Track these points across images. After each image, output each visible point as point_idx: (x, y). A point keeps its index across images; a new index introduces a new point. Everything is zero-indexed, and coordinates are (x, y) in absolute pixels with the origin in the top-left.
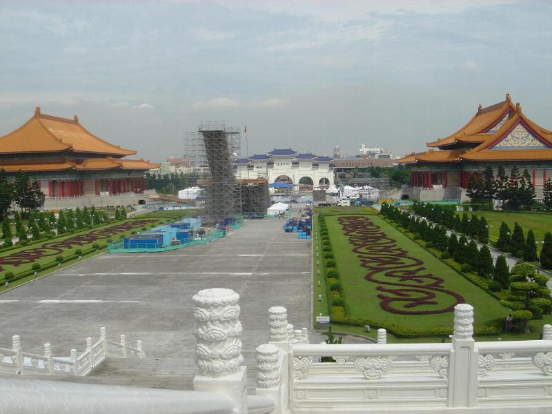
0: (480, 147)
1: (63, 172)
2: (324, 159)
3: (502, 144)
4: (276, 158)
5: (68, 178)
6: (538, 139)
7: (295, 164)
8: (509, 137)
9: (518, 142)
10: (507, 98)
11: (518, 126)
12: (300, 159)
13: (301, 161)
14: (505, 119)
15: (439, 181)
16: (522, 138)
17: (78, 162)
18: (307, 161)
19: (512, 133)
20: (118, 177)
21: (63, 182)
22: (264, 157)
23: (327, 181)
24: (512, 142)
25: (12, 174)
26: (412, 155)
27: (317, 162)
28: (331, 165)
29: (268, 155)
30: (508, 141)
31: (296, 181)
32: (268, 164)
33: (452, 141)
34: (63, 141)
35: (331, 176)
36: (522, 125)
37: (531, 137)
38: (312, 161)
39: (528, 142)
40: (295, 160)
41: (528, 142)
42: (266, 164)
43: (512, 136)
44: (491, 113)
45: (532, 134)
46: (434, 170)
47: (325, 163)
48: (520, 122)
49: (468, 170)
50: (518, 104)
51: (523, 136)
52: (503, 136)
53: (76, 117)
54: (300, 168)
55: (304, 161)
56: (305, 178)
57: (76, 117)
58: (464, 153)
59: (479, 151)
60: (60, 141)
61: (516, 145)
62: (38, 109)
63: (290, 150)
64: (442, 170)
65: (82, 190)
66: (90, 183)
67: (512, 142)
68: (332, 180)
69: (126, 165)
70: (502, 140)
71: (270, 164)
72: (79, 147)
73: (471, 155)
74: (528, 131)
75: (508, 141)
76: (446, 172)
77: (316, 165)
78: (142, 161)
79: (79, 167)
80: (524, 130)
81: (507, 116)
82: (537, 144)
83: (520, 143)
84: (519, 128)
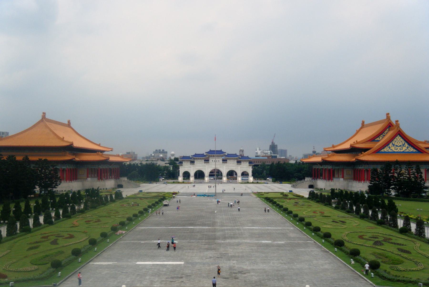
3: (386, 149)
4: (211, 156)
5: (67, 167)
7: (225, 161)
8: (391, 145)
10: (387, 116)
11: (397, 137)
13: (229, 159)
14: (386, 132)
16: (400, 146)
18: (233, 159)
19: (393, 142)
20: (104, 167)
21: (63, 170)
22: (203, 155)
24: (393, 148)
25: (33, 162)
27: (240, 159)
28: (250, 163)
30: (390, 148)
31: (225, 173)
32: (205, 161)
34: (65, 139)
35: (250, 170)
36: (400, 136)
37: (406, 145)
38: (236, 159)
39: (404, 148)
41: (404, 148)
42: (203, 160)
43: (393, 144)
45: (407, 142)
46: (330, 167)
47: (246, 161)
48: (399, 134)
49: (357, 168)
51: (401, 144)
52: (387, 144)
54: (228, 164)
55: (231, 159)
56: (230, 171)
58: (358, 155)
60: (63, 139)
62: (44, 113)
63: (221, 151)
66: (83, 172)
67: (393, 148)
68: (250, 173)
70: (386, 147)
71: (207, 161)
75: (390, 148)
77: (239, 162)
78: (118, 156)
79: (77, 159)
80: (402, 140)
81: (388, 129)
82: (412, 149)
83: (399, 149)
84: (399, 138)
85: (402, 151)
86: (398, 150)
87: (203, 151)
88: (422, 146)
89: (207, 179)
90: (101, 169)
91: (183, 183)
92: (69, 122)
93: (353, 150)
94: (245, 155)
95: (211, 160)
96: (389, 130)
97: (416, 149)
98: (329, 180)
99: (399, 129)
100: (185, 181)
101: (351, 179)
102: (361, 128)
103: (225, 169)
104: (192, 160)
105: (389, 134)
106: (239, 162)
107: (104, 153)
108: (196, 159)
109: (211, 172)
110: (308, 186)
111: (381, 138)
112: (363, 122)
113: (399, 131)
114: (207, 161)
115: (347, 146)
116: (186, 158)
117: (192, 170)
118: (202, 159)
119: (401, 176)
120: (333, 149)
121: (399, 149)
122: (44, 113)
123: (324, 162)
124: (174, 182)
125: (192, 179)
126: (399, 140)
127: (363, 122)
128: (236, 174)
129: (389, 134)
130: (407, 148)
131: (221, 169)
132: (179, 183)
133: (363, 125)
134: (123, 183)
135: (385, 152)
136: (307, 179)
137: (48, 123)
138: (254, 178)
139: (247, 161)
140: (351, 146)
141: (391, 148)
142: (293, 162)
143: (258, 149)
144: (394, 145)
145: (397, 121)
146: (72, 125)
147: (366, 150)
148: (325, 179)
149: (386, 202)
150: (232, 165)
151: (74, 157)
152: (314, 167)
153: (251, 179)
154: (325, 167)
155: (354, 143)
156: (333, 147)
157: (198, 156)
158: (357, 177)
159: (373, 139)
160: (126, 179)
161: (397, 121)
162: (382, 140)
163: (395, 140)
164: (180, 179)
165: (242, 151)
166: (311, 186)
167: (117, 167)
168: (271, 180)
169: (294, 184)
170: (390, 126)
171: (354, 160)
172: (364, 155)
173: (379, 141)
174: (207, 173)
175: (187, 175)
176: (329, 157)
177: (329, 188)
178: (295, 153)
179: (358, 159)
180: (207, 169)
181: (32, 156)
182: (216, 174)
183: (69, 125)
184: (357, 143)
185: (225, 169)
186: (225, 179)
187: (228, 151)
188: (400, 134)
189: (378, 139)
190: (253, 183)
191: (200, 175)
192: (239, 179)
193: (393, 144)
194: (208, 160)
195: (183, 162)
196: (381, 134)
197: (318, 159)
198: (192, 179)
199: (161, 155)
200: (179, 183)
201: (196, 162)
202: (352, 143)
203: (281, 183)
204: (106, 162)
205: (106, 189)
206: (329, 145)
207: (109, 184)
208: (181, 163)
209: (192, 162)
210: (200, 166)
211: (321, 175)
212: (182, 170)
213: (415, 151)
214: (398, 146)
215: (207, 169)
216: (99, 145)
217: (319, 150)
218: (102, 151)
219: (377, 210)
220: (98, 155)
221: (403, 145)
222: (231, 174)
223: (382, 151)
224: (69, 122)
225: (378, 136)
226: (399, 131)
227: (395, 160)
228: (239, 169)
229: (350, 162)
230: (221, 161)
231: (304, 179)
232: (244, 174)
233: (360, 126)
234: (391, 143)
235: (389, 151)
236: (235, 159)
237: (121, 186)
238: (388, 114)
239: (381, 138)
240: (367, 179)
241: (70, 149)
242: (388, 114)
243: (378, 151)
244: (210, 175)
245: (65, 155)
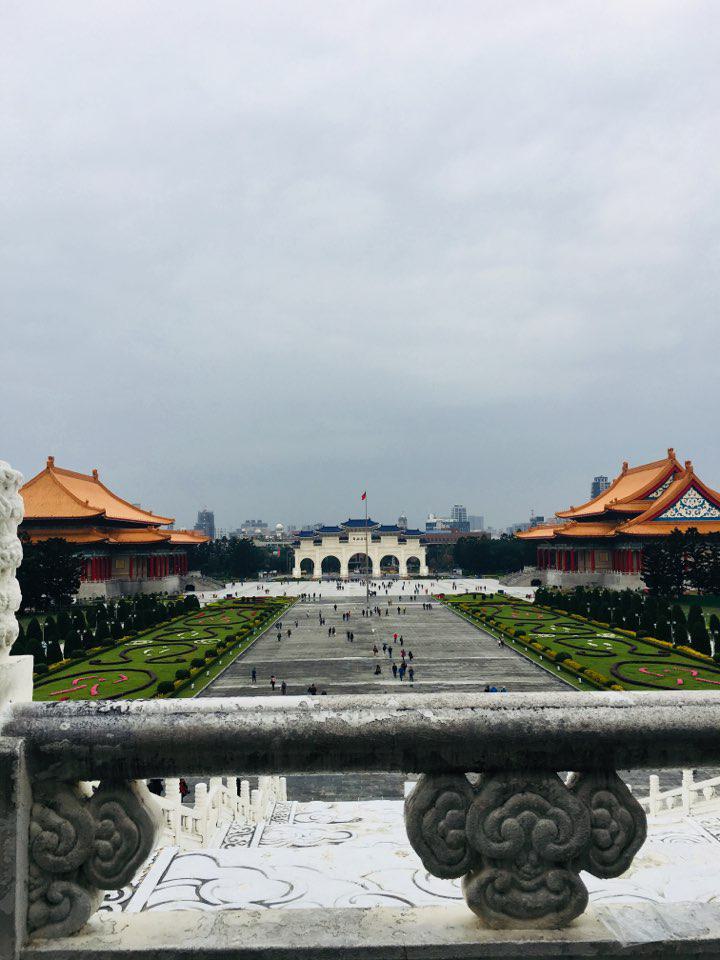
2: (414, 533)
3: (669, 514)
7: (376, 539)
8: (678, 505)
12: (379, 532)
14: (668, 482)
16: (696, 507)
17: (111, 533)
21: (88, 559)
23: (417, 562)
24: (683, 512)
27: (403, 534)
28: (421, 542)
29: (340, 527)
34: (90, 505)
35: (421, 554)
37: (707, 504)
40: (376, 533)
43: (682, 504)
45: (708, 501)
51: (697, 504)
52: (671, 504)
53: (95, 472)
57: (95, 472)
60: (85, 505)
61: (688, 516)
65: (110, 571)
67: (683, 512)
69: (175, 538)
71: (344, 539)
72: (111, 513)
74: (704, 497)
77: (402, 541)
80: (698, 496)
83: (693, 513)
84: (692, 492)
86: (693, 515)
87: (337, 522)
90: (155, 558)
91: (302, 579)
93: (610, 516)
94: (409, 528)
95: (351, 536)
96: (674, 479)
98: (567, 569)
100: (306, 577)
101: (608, 569)
102: (623, 476)
103: (376, 553)
104: (316, 535)
105: (675, 486)
106: (402, 541)
107: (160, 528)
108: (326, 536)
109: (351, 560)
110: (529, 583)
112: (626, 465)
113: (693, 480)
114: (344, 539)
115: (598, 507)
117: (317, 555)
118: (336, 535)
119: (702, 562)
120: (572, 514)
121: (693, 513)
122: (51, 458)
123: (559, 539)
124: (286, 580)
125: (318, 572)
126: (692, 498)
127: (626, 465)
128: (397, 562)
129: (675, 486)
130: (709, 510)
131: (370, 554)
132: (294, 580)
133: (626, 471)
134: (195, 584)
135: (668, 519)
136: (526, 569)
137: (57, 476)
138: (430, 569)
139: (417, 538)
140: (606, 508)
141: (679, 511)
142: (496, 537)
143: (431, 516)
144: (684, 506)
145: (688, 463)
148: (560, 569)
149: (686, 611)
150: (389, 546)
151: (107, 536)
152: (539, 548)
153: (424, 570)
155: (611, 502)
156: (573, 510)
158: (620, 564)
159: (645, 496)
160: (198, 574)
161: (688, 463)
162: (662, 497)
163: (686, 496)
164: (297, 572)
165: (404, 520)
166: (535, 583)
167: (183, 553)
168: (460, 572)
169: (505, 578)
170: (674, 471)
171: (613, 533)
173: (656, 499)
175: (308, 565)
176: (567, 529)
177: (569, 586)
178: (497, 521)
179: (620, 533)
180: (344, 553)
181: (69, 535)
182: (360, 563)
183: (95, 478)
184: (618, 502)
185: (376, 553)
186: (377, 570)
187: (383, 520)
188: (695, 484)
189: (654, 495)
190: (428, 577)
191: (331, 565)
194: (347, 539)
195: (302, 542)
196: (661, 486)
197: (549, 533)
198: (318, 572)
199: (259, 531)
200: (294, 580)
202: (608, 503)
203: (480, 577)
204: (165, 544)
205: (166, 593)
206: (564, 508)
207: (171, 583)
208: (297, 544)
209: (318, 542)
210: (331, 547)
211: (553, 563)
214: (691, 508)
216: (150, 514)
217: (549, 515)
218: (157, 525)
219: (669, 623)
220: (150, 531)
221: (701, 506)
222: (388, 562)
223: (663, 516)
225: (654, 489)
226: (693, 480)
227: (707, 532)
229: (605, 537)
230: (369, 538)
231: (522, 569)
233: (621, 472)
236: (395, 535)
237: (192, 588)
238: (671, 450)
240: (638, 569)
241: (100, 521)
242: (671, 450)
243: (655, 518)
244: (351, 566)
245: (88, 534)
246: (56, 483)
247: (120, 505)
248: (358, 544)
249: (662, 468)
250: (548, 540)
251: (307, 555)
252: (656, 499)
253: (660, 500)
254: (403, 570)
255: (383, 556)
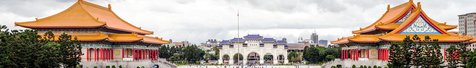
0: (392, 32)
1: (98, 42)
3: (408, 30)
6: (433, 27)
8: (413, 26)
9: (419, 29)
11: (419, 19)
14: (409, 14)
15: (362, 56)
16: (422, 27)
19: (415, 23)
24: (415, 29)
26: (343, 39)
30: (412, 29)
33: (373, 28)
43: (414, 25)
44: (400, 9)
48: (421, 15)
50: (419, 3)
51: (422, 25)
59: (391, 35)
64: (366, 48)
67: (415, 29)
73: (386, 37)
76: (368, 49)
80: (423, 21)
82: (433, 30)
83: (420, 30)
84: (420, 19)
85: (423, 32)
86: (420, 31)
88: (442, 28)
89: (245, 61)
92: (109, 5)
96: (412, 13)
97: (436, 30)
99: (420, 10)
103: (262, 52)
111: (404, 20)
116: (224, 43)
117: (231, 53)
121: (420, 30)
129: (411, 16)
130: (428, 29)
146: (112, 9)
147: (390, 31)
153: (286, 61)
154: (352, 48)
157: (236, 40)
159: (396, 21)
163: (417, 21)
172: (387, 36)
174: (245, 57)
180: (245, 52)
186: (262, 61)
189: (401, 21)
191: (238, 58)
192: (276, 61)
193: (414, 25)
198: (231, 61)
201: (236, 45)
208: (221, 46)
209: (232, 46)
210: (238, 49)
212: (221, 54)
213: (435, 31)
215: (245, 52)
221: (424, 26)
224: (109, 5)
228: (276, 53)
230: (258, 44)
232: (281, 57)
234: (413, 24)
235: (411, 31)
239: (404, 20)
246: (83, 10)
247: (128, 26)
248: (253, 47)
249: (405, 7)
250: (346, 44)
251: (226, 53)
252: (402, 22)
253: (403, 23)
254: (276, 61)
255: (265, 54)
